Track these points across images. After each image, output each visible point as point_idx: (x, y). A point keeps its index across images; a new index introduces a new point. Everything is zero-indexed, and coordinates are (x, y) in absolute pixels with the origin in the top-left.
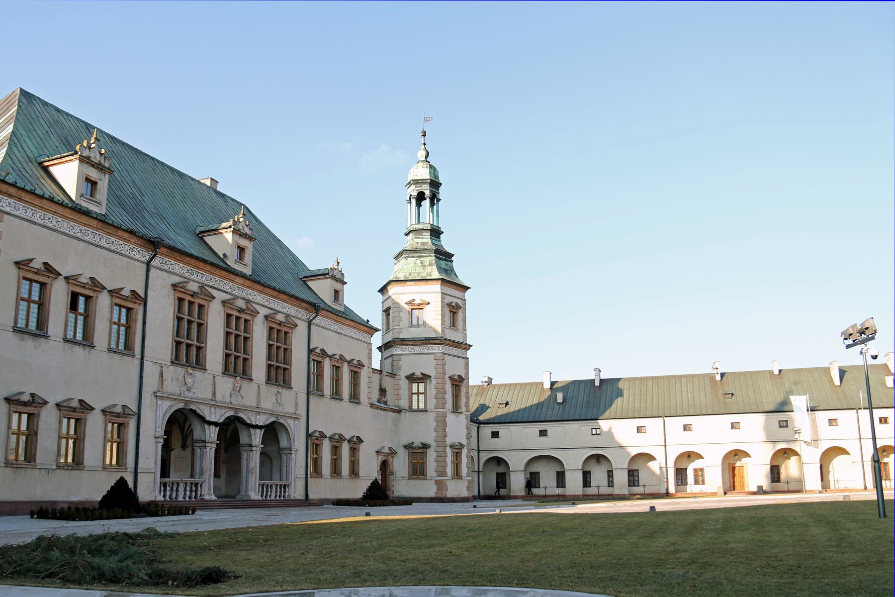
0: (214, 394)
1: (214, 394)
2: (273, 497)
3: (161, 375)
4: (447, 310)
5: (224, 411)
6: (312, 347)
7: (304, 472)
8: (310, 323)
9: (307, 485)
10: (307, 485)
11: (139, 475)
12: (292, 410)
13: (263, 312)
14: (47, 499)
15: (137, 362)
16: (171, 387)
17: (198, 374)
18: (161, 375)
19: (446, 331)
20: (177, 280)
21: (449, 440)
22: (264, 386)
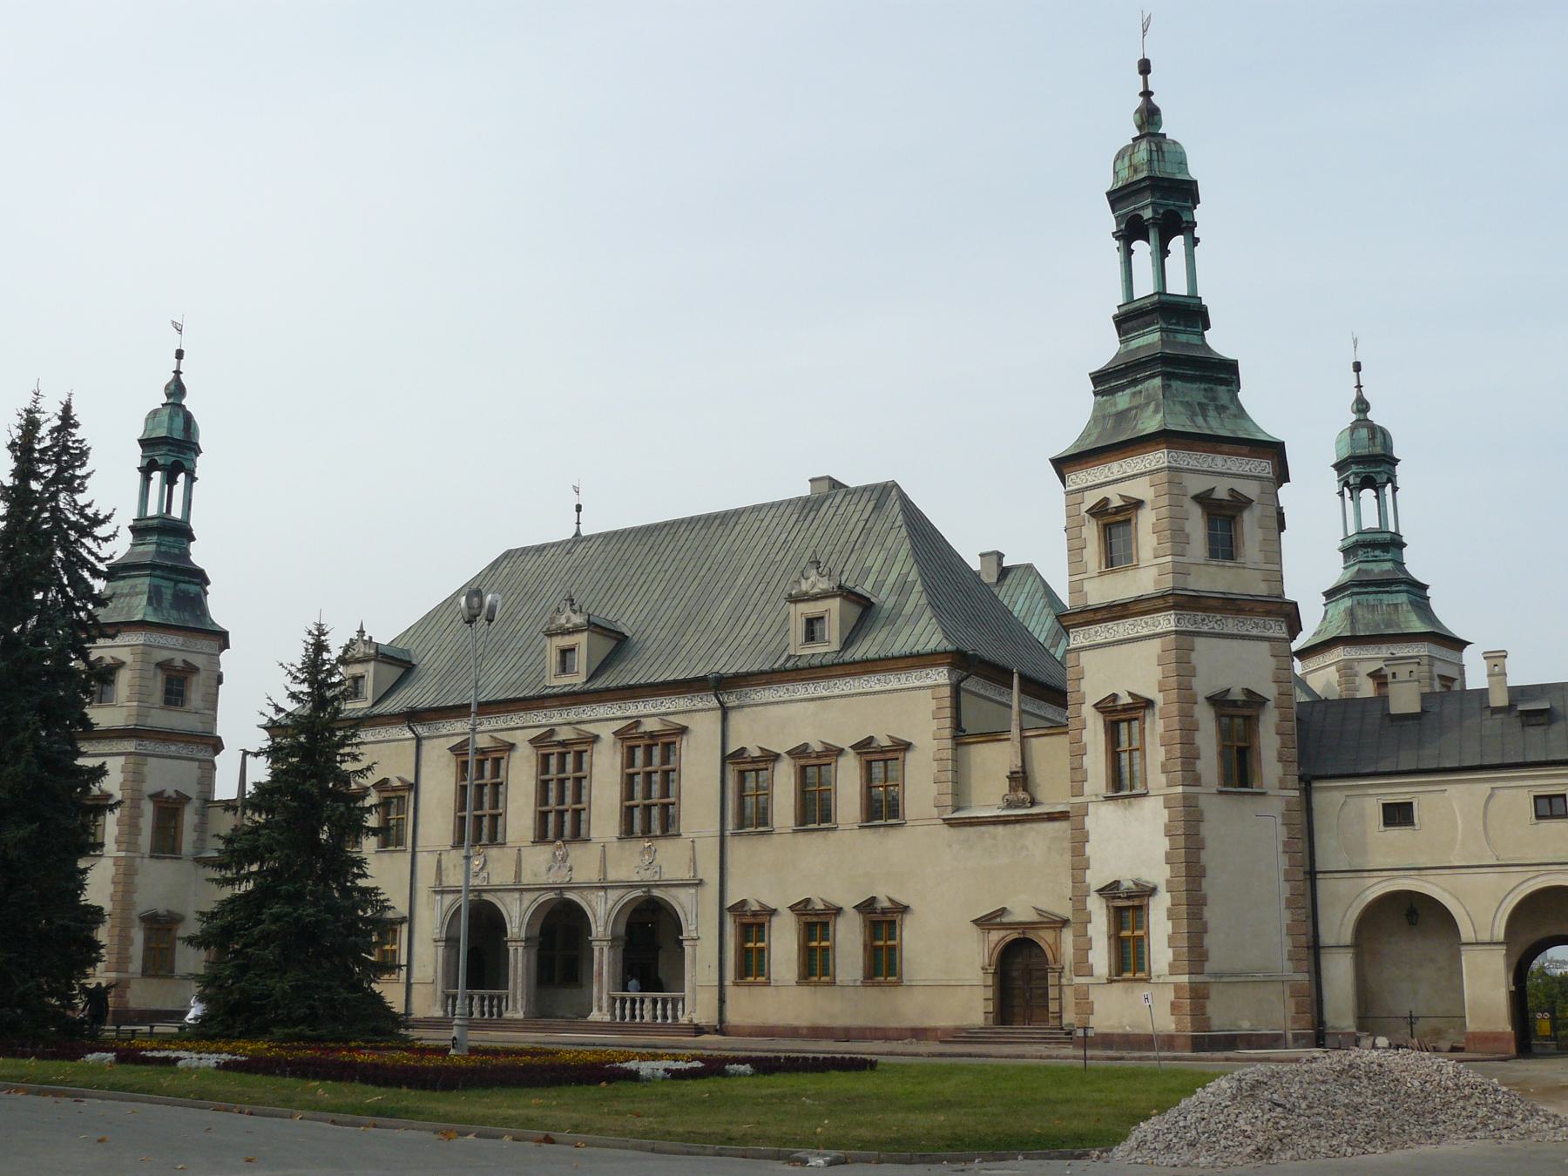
0: (518, 874)
1: (518, 874)
2: (647, 1018)
3: (439, 862)
4: (1091, 531)
5: (537, 894)
6: (732, 748)
7: (716, 977)
8: (725, 711)
9: (722, 1001)
10: (722, 1001)
11: (415, 988)
12: (685, 874)
13: (606, 732)
14: (143, 1008)
15: (408, 856)
16: (454, 878)
17: (493, 852)
18: (439, 862)
19: (1087, 586)
20: (458, 740)
21: (1096, 878)
22: (614, 849)
